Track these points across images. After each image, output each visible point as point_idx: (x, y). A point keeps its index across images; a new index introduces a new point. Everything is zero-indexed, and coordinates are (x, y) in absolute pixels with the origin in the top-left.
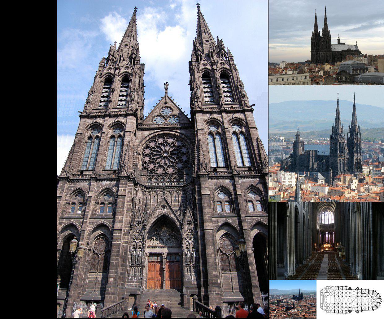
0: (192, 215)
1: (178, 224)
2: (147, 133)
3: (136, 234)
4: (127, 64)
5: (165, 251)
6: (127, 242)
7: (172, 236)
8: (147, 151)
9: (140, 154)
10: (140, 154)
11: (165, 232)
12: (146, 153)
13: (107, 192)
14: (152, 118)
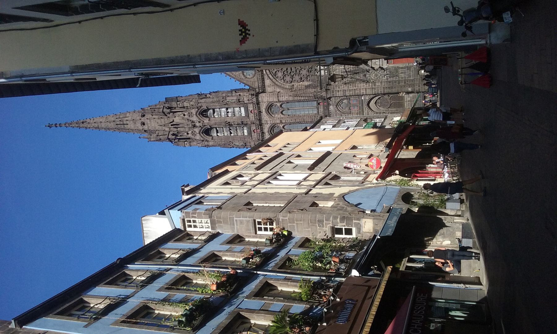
2: (267, 82)
4: (184, 115)
6: (381, 82)
8: (288, 78)
9: (293, 85)
10: (293, 85)
12: (291, 80)
14: (247, 79)
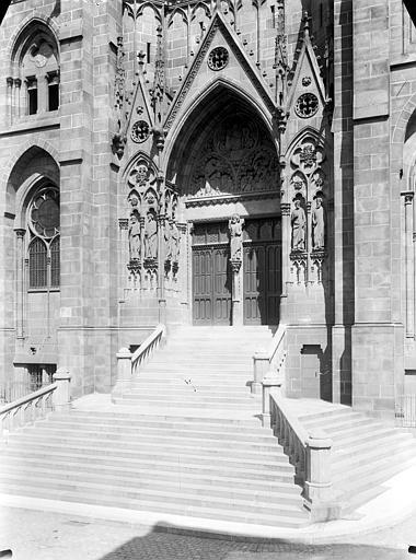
0: (318, 73)
1: (268, 116)
3: (137, 168)
5: (236, 211)
7: (261, 158)
11: (235, 153)
13: (38, 37)
